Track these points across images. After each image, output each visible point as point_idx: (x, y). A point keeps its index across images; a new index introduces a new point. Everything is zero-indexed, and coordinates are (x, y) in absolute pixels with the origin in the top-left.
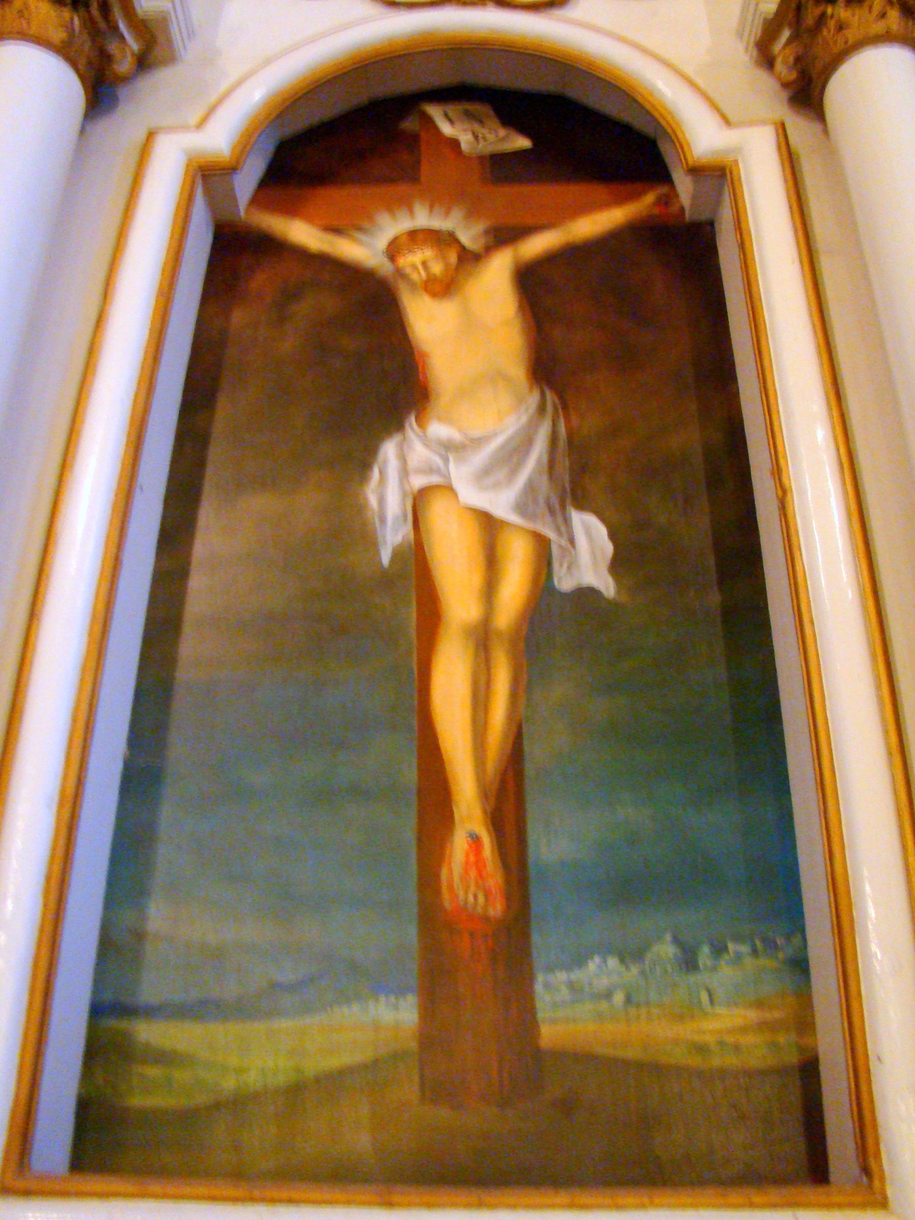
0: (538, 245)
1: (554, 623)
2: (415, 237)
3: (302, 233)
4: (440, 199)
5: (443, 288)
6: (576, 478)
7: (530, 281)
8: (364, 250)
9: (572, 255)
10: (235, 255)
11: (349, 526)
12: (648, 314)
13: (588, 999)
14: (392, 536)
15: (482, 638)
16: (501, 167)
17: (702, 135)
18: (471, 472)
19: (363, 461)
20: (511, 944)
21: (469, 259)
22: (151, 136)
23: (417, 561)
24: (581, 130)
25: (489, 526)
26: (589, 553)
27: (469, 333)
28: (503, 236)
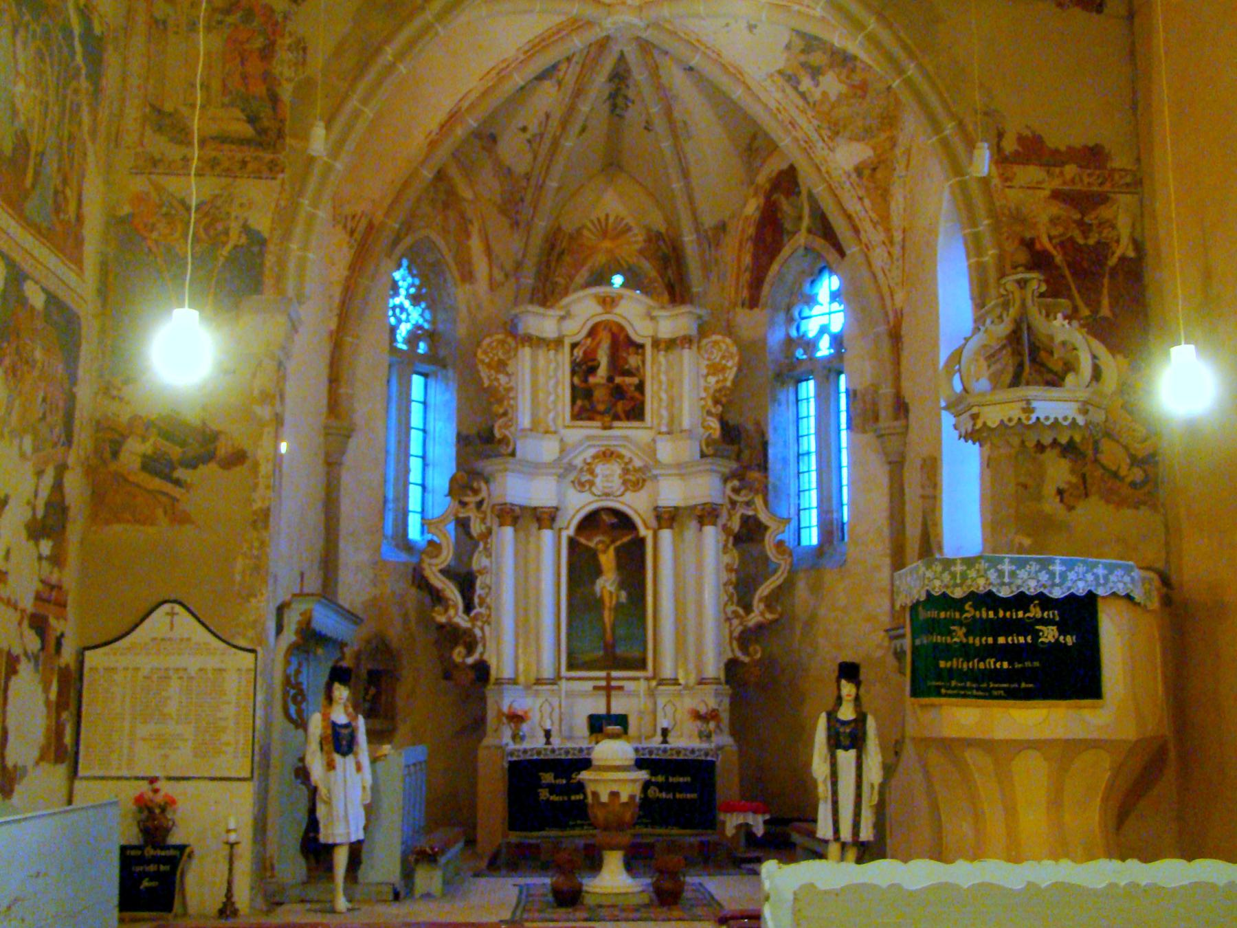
0: (618, 543)
1: (619, 607)
2: (600, 542)
3: (583, 541)
4: (604, 533)
5: (604, 552)
6: (622, 585)
7: (617, 551)
8: (592, 544)
9: (623, 546)
10: (572, 543)
11: (594, 595)
12: (633, 560)
13: (621, 651)
14: (598, 594)
15: (610, 609)
16: (613, 526)
17: (643, 532)
18: (607, 584)
19: (593, 583)
20: (613, 647)
21: (608, 547)
22: (560, 530)
23: (602, 597)
24: (623, 522)
25: (611, 593)
26: (623, 595)
27: (607, 560)
28: (613, 542)
